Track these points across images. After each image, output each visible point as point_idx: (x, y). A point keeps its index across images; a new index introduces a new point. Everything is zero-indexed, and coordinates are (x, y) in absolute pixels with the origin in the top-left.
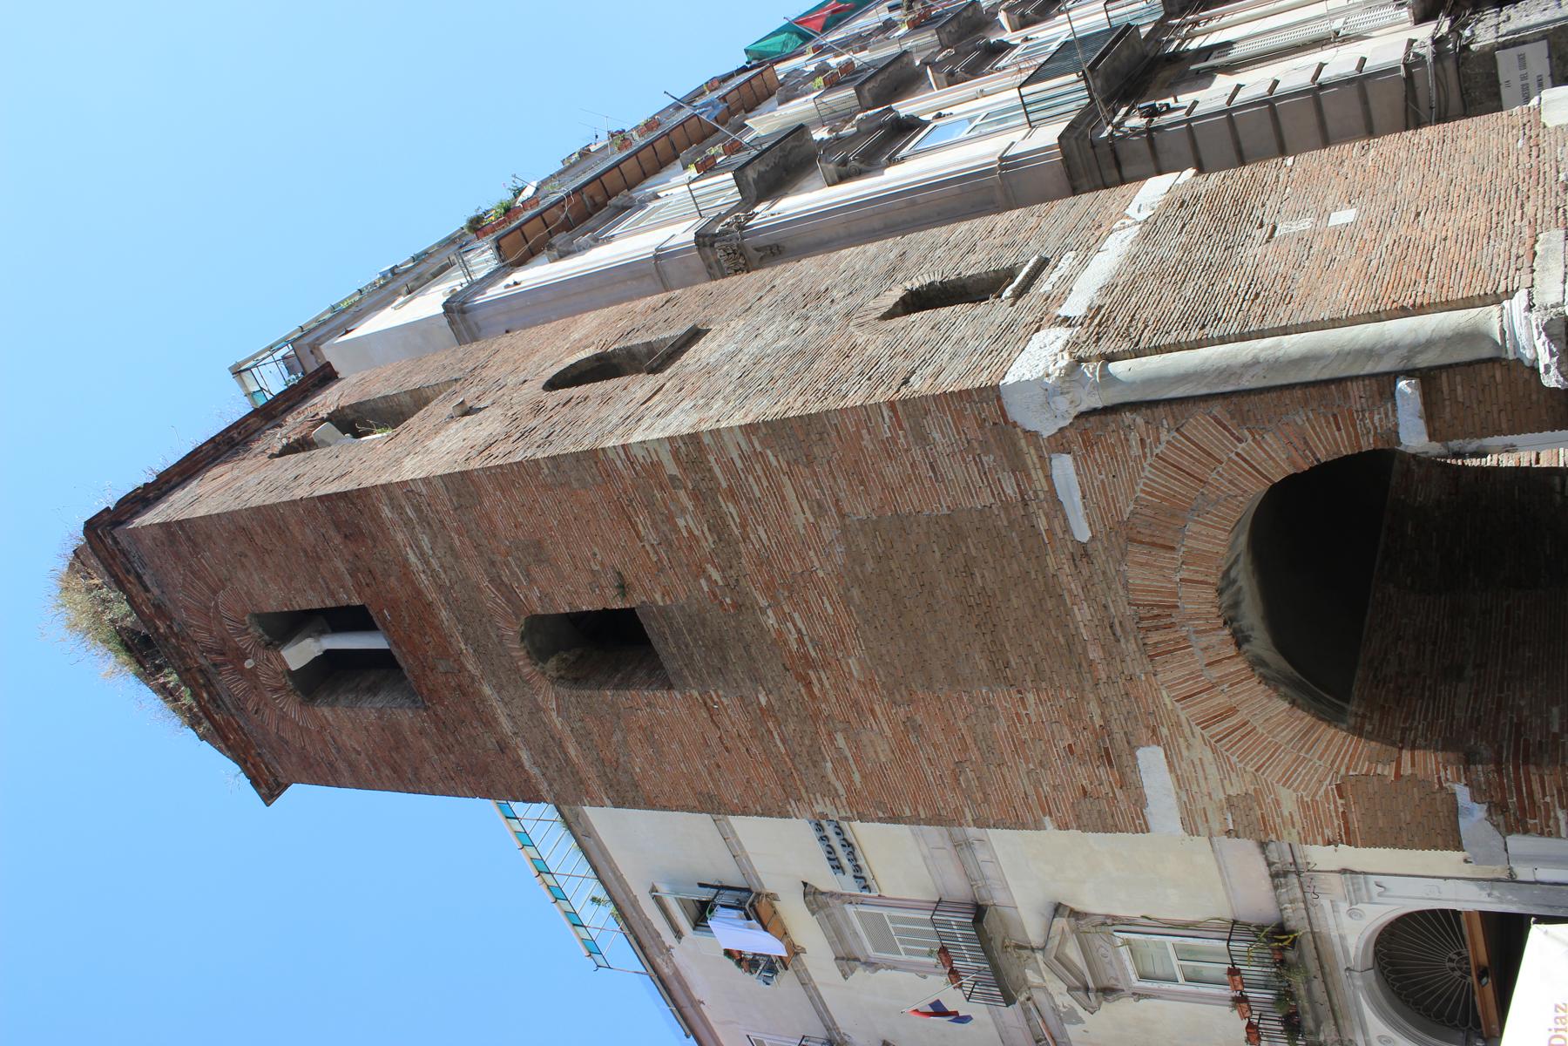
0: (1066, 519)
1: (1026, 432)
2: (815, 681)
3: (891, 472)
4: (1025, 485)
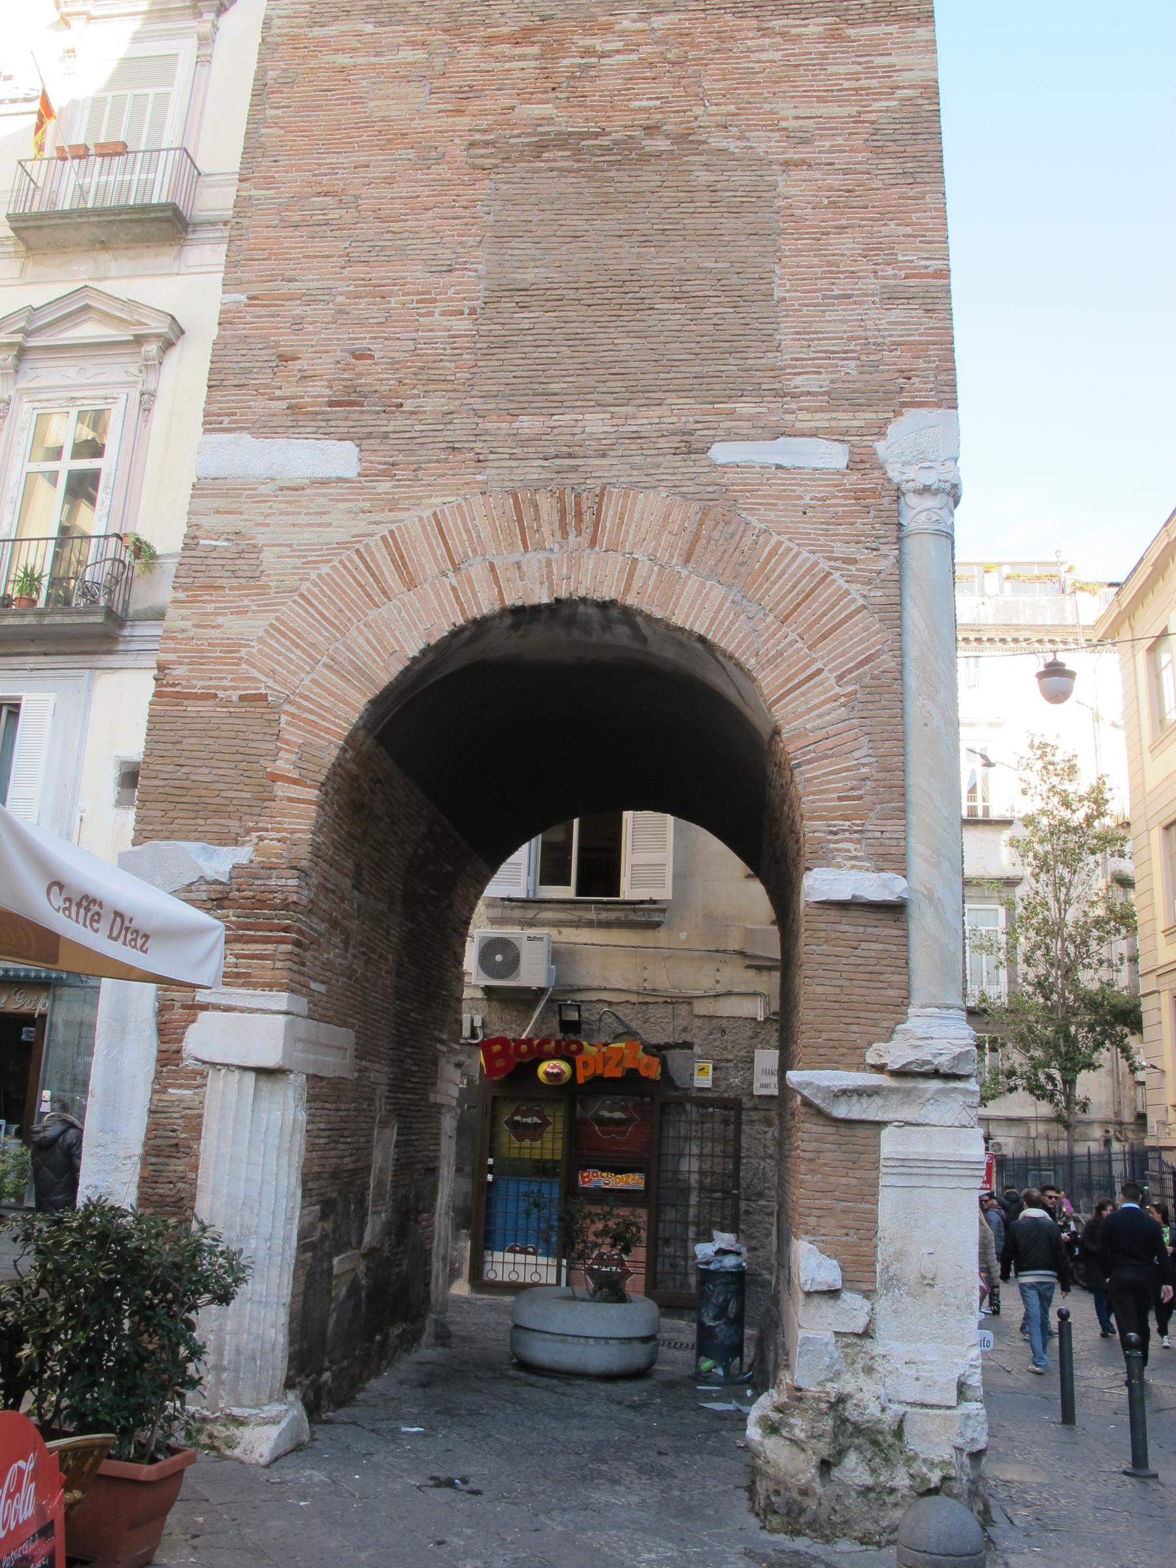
0: (747, 438)
1: (887, 421)
2: (519, 51)
3: (847, 244)
4: (806, 402)
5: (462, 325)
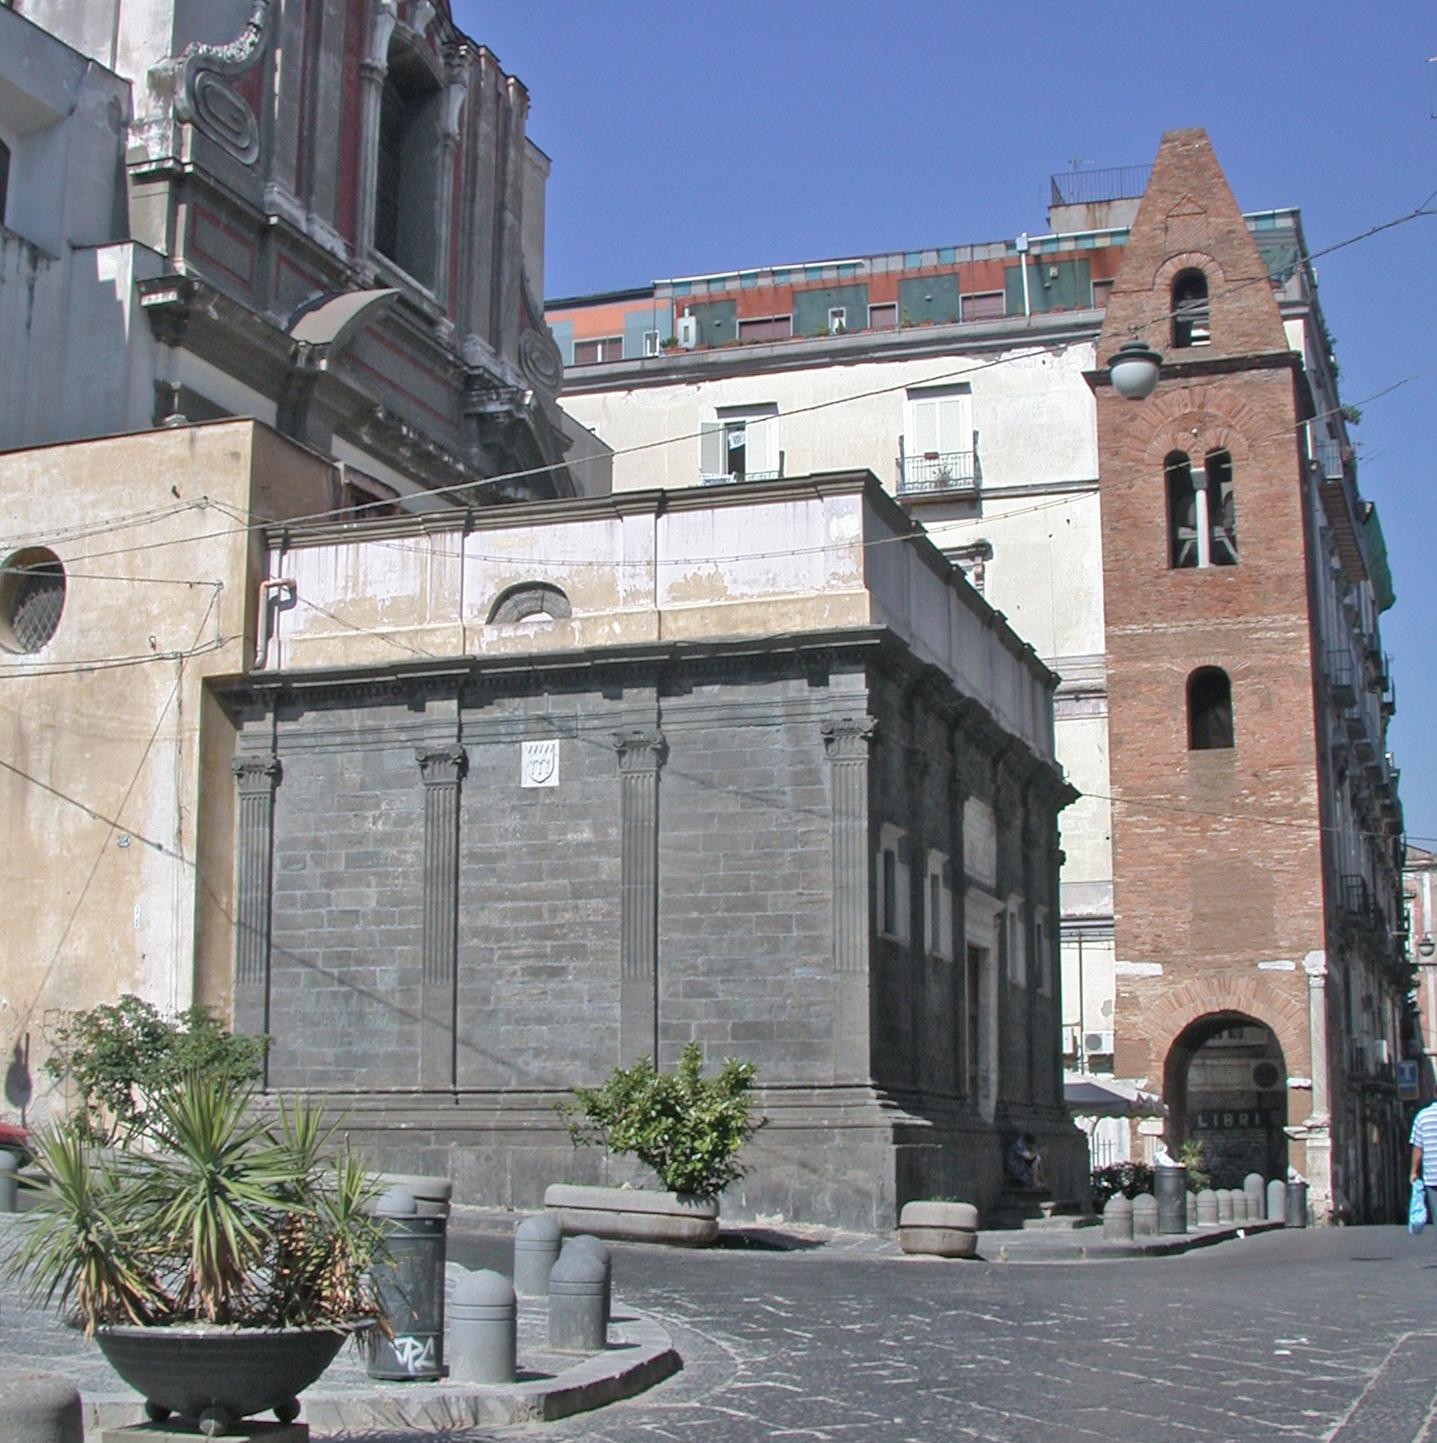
5: (1187, 926)
